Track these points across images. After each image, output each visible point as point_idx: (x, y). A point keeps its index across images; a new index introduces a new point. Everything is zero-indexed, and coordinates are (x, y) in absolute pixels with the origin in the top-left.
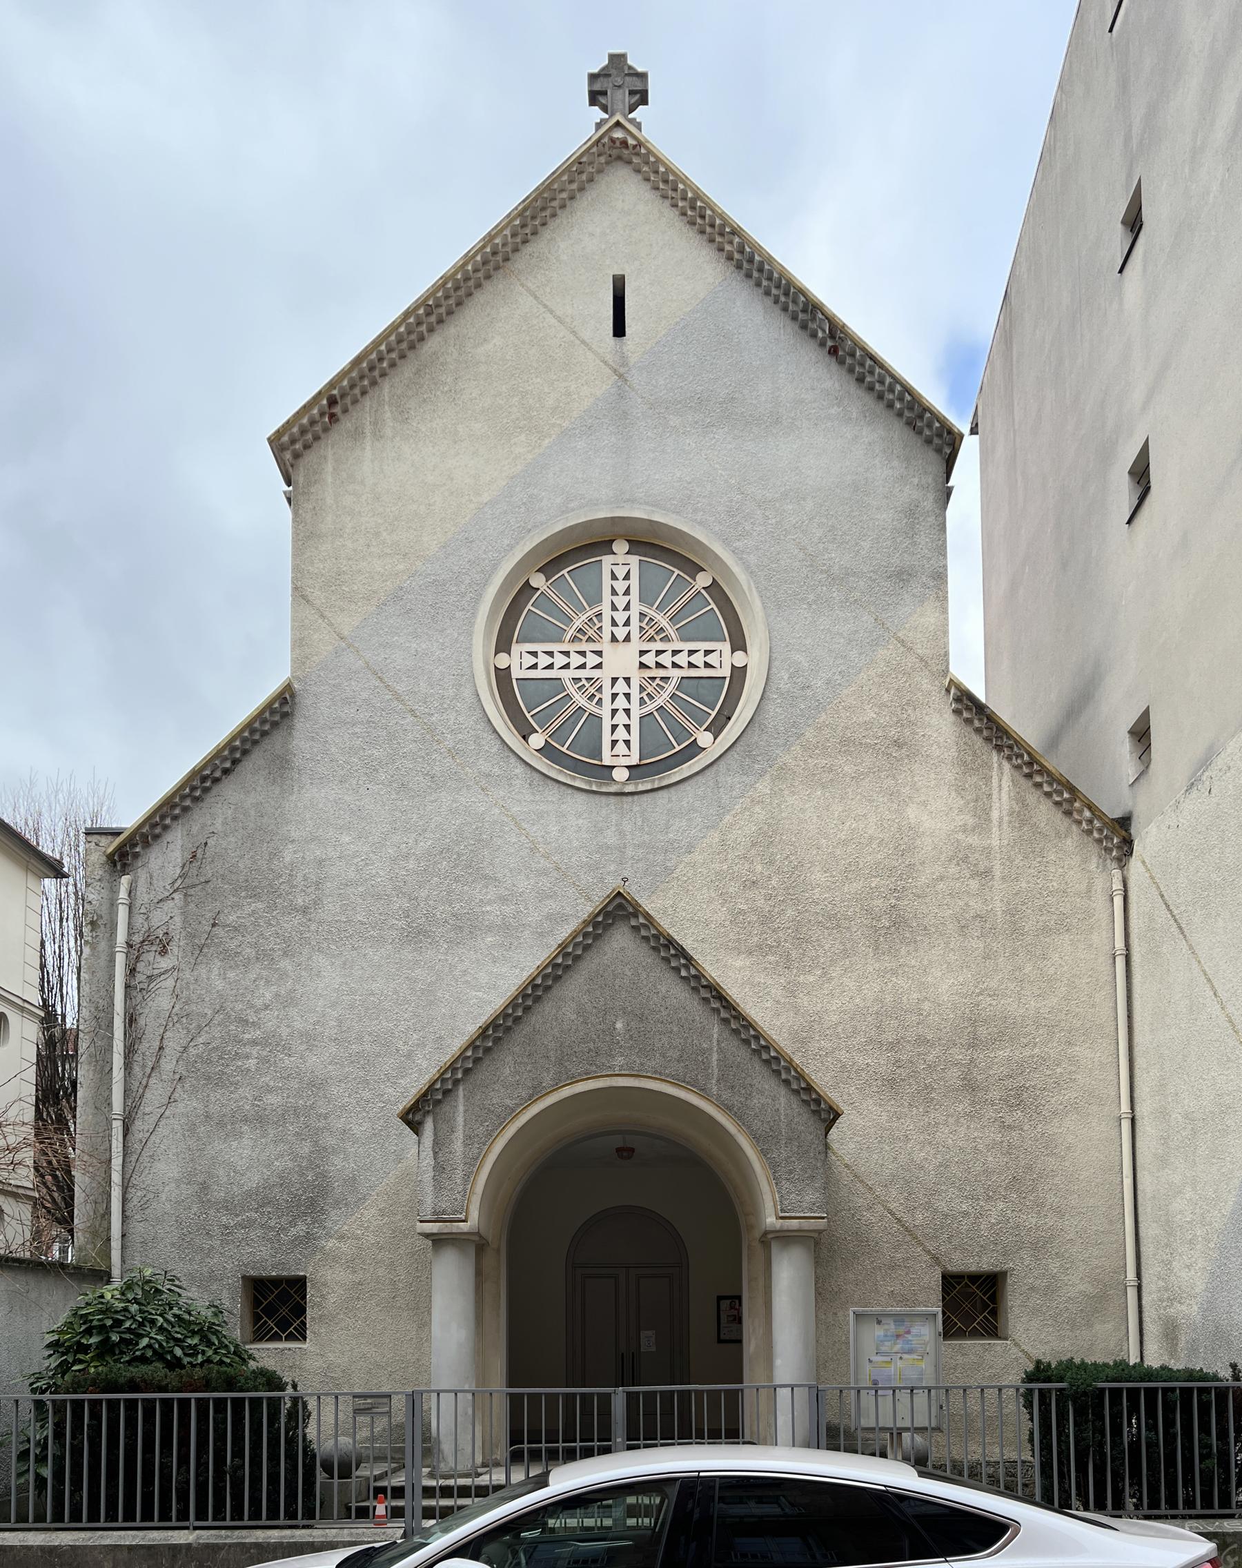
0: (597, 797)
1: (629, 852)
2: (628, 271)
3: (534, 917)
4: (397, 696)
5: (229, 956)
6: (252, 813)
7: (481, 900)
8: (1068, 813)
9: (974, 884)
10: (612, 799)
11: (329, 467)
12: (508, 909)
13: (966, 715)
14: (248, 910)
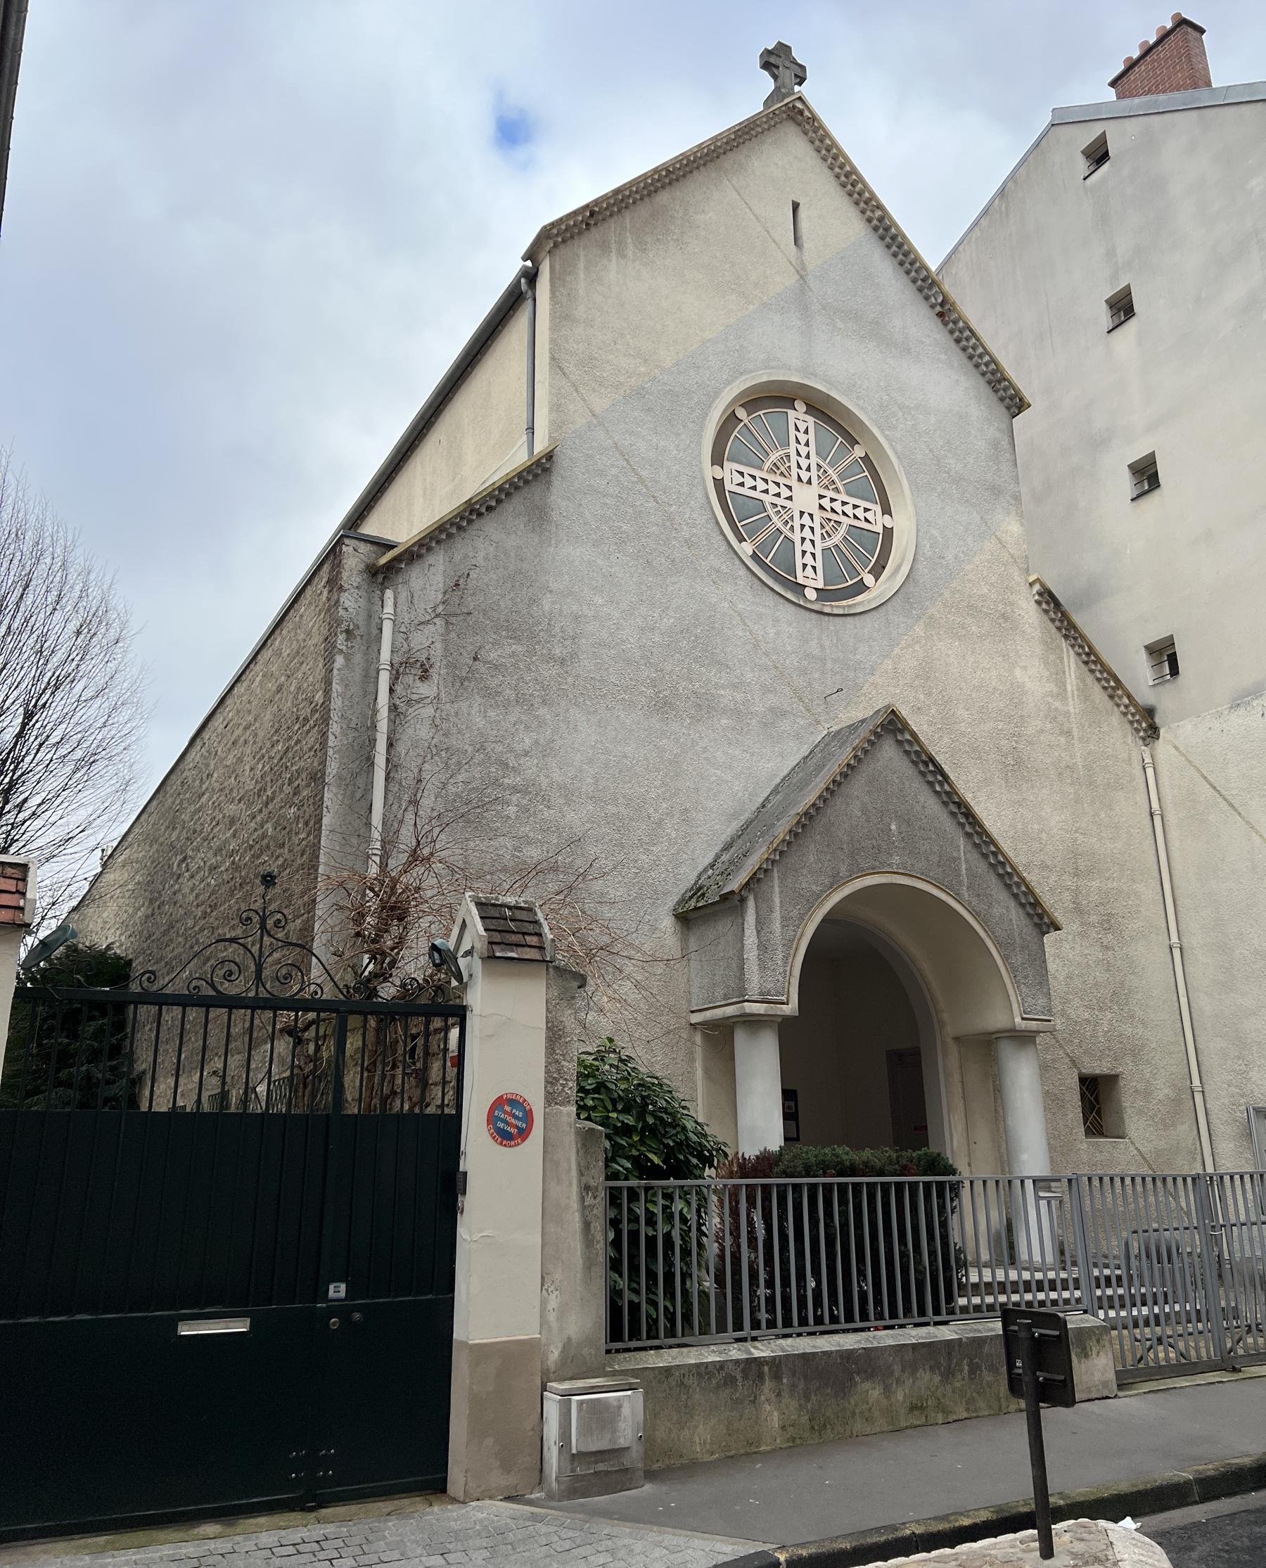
0: (803, 611)
1: (829, 665)
2: (801, 201)
3: (759, 708)
4: (641, 480)
5: (490, 694)
6: (513, 555)
7: (716, 684)
8: (1111, 697)
9: (1062, 740)
10: (814, 616)
11: (581, 265)
12: (739, 697)
13: (1044, 606)
14: (508, 650)
